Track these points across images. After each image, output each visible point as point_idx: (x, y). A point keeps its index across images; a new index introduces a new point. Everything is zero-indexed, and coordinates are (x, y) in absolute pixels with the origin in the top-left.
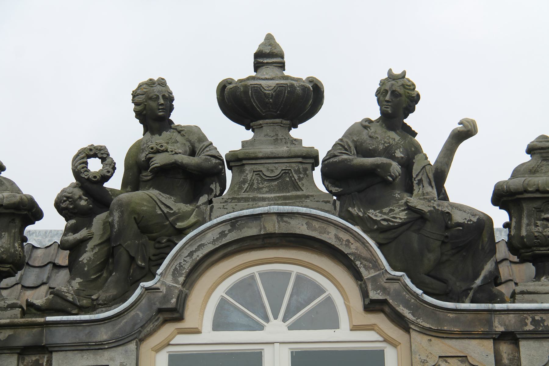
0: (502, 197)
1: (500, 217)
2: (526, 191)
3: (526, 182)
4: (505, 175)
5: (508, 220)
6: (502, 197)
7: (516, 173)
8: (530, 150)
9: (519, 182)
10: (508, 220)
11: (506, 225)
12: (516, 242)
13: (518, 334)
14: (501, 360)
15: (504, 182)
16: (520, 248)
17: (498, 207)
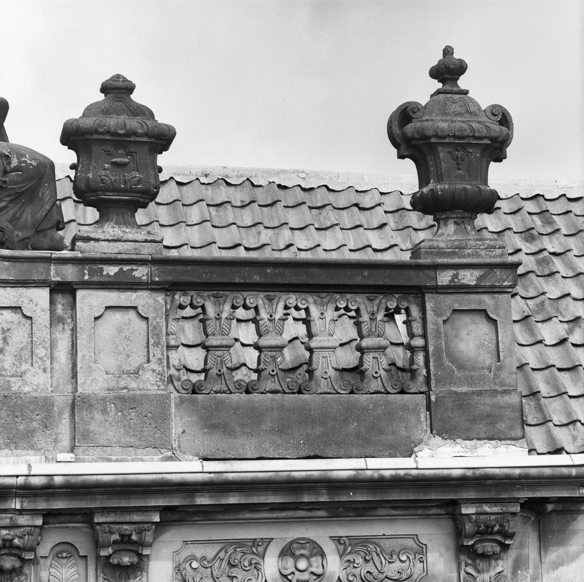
0: (72, 136)
1: (64, 159)
2: (96, 132)
3: (97, 122)
4: (76, 113)
5: (75, 161)
6: (72, 136)
7: (89, 111)
8: (105, 89)
9: (90, 122)
10: (75, 161)
11: (73, 167)
12: (83, 186)
13: (76, 284)
14: (55, 310)
15: (76, 120)
16: (85, 194)
17: (67, 147)
